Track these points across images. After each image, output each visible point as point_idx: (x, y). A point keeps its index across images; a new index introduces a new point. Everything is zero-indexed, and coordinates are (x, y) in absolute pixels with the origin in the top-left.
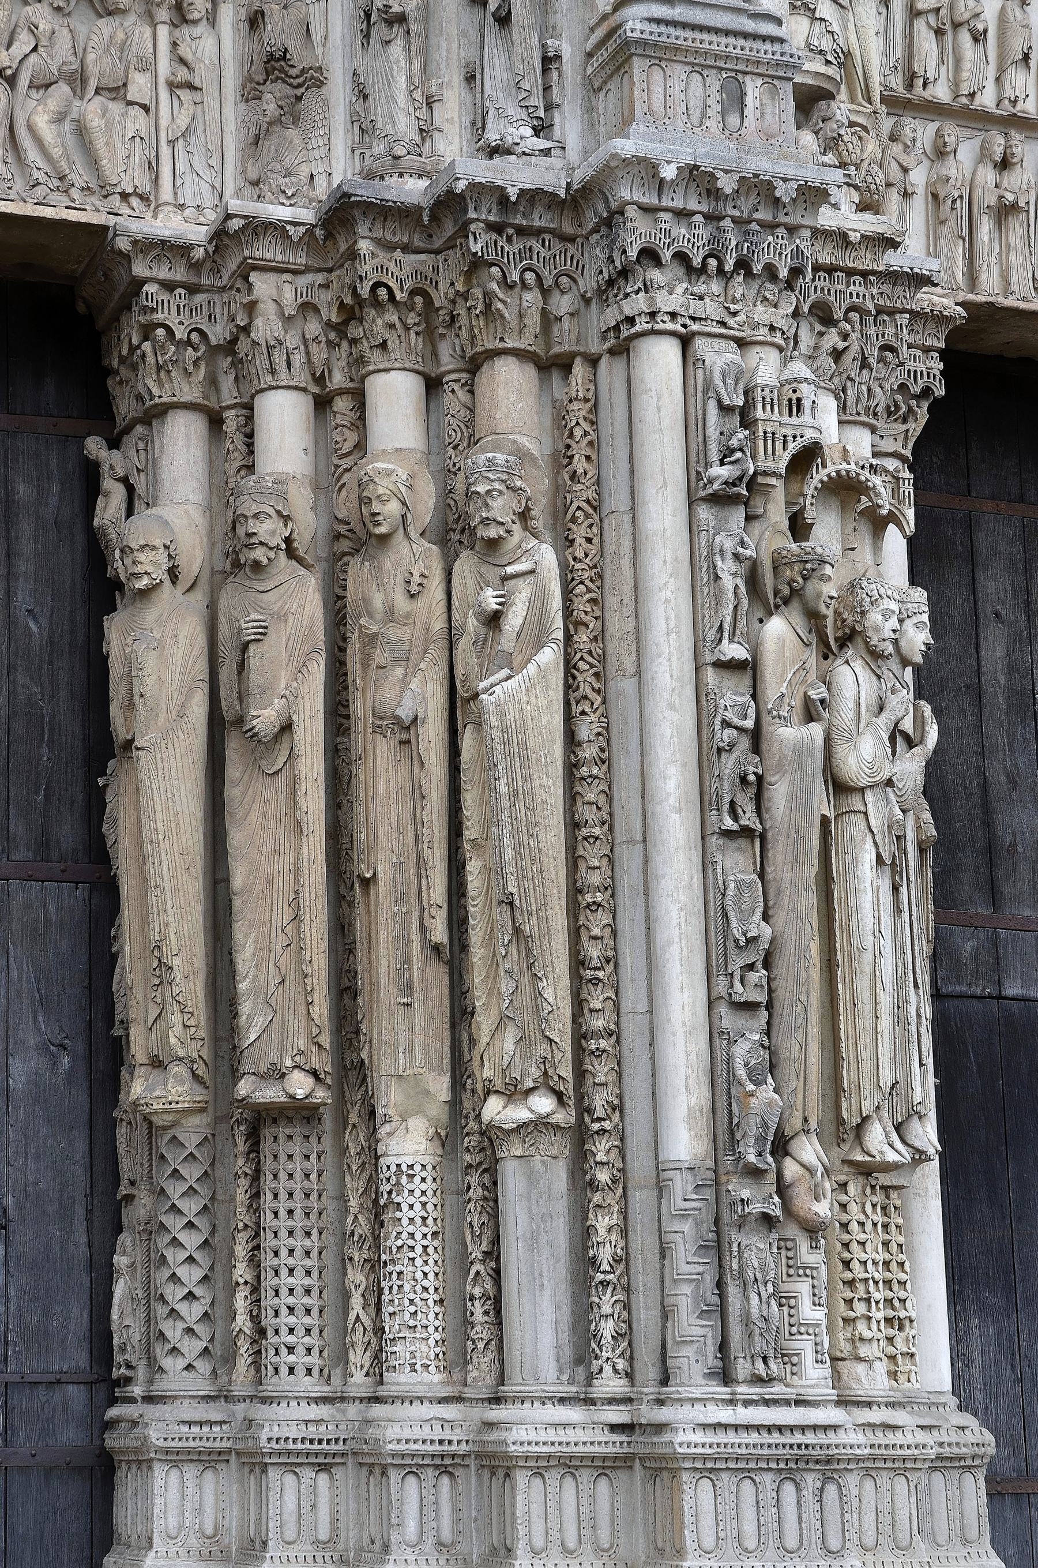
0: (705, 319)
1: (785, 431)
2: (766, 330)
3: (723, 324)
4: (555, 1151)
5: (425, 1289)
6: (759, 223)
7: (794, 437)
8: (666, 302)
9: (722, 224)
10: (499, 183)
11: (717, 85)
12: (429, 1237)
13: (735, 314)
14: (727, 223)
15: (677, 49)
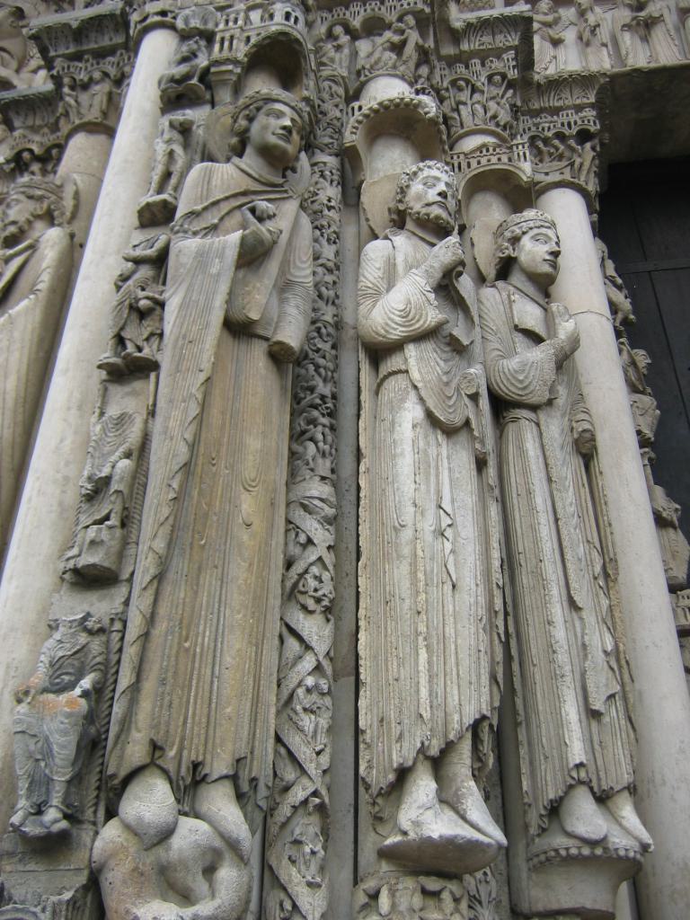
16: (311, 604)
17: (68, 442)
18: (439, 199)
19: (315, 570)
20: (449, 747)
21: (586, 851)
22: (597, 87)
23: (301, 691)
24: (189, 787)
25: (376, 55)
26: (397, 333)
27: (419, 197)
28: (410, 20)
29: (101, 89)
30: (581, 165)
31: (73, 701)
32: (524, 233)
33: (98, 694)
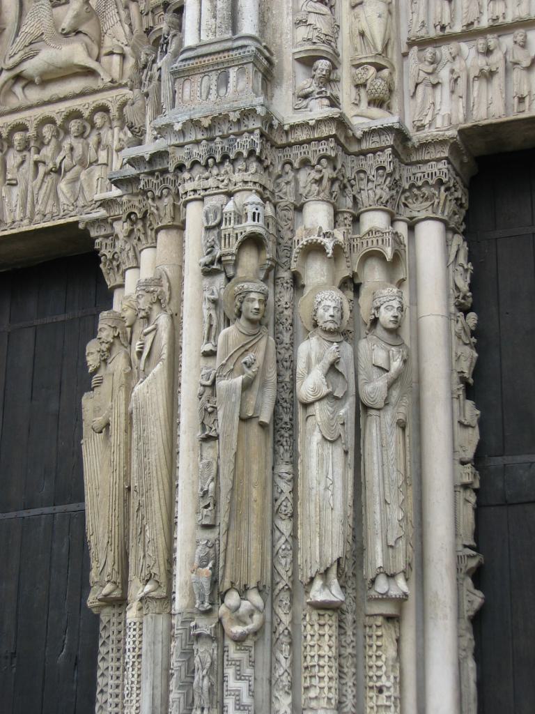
0: (210, 188)
1: (236, 232)
2: (241, 184)
3: (218, 187)
4: (157, 611)
5: (132, 682)
6: (233, 134)
7: (241, 233)
8: (189, 186)
9: (216, 140)
10: (141, 154)
11: (215, 78)
12: (136, 657)
13: (223, 181)
14: (218, 140)
15: (194, 69)
16: (283, 517)
17: (191, 466)
18: (330, 318)
19: (284, 503)
20: (327, 571)
21: (380, 597)
22: (449, 144)
23: (280, 551)
24: (243, 592)
25: (308, 189)
26: (311, 399)
27: (322, 317)
28: (324, 161)
29: (167, 201)
30: (439, 203)
31: (207, 570)
32: (381, 305)
33: (215, 566)
